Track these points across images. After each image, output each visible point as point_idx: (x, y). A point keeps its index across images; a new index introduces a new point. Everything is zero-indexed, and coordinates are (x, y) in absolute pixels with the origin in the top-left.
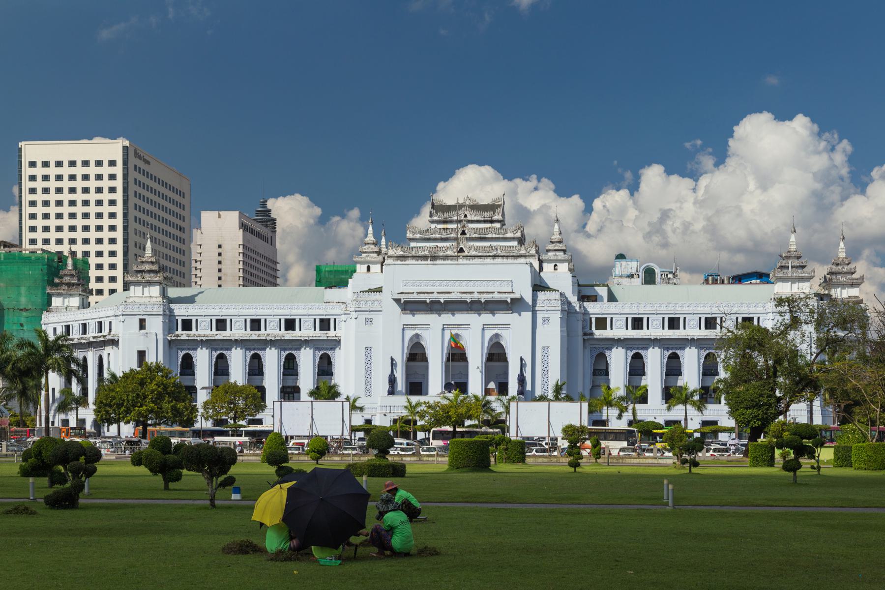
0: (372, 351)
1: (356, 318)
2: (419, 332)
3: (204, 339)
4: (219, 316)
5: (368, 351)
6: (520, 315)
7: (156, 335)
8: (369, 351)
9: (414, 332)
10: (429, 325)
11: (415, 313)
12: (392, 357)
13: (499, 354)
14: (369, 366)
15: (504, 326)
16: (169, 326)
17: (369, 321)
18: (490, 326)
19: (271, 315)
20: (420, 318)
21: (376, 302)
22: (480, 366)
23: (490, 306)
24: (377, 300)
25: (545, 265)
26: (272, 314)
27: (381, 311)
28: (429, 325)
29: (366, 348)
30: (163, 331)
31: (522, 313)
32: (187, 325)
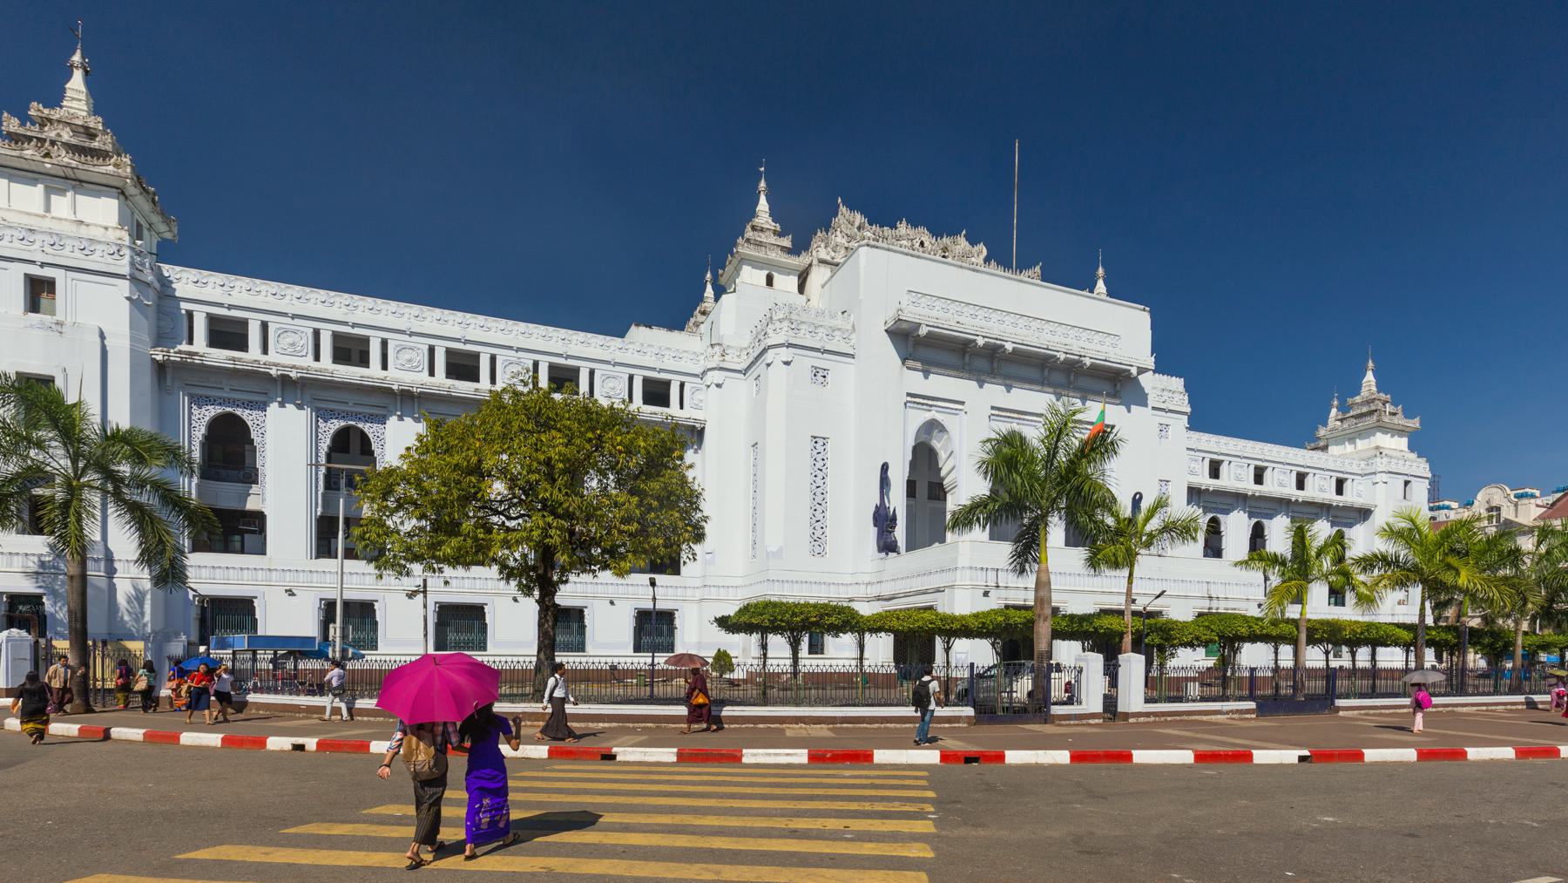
1: (787, 363)
2: (939, 417)
3: (292, 375)
4: (345, 323)
7: (102, 336)
8: (820, 448)
9: (928, 416)
10: (962, 403)
11: (934, 369)
16: (158, 327)
17: (819, 374)
19: (510, 348)
20: (942, 384)
21: (837, 333)
23: (1083, 382)
24: (839, 329)
26: (515, 344)
27: (852, 356)
28: (962, 403)
30: (131, 328)
32: (228, 333)
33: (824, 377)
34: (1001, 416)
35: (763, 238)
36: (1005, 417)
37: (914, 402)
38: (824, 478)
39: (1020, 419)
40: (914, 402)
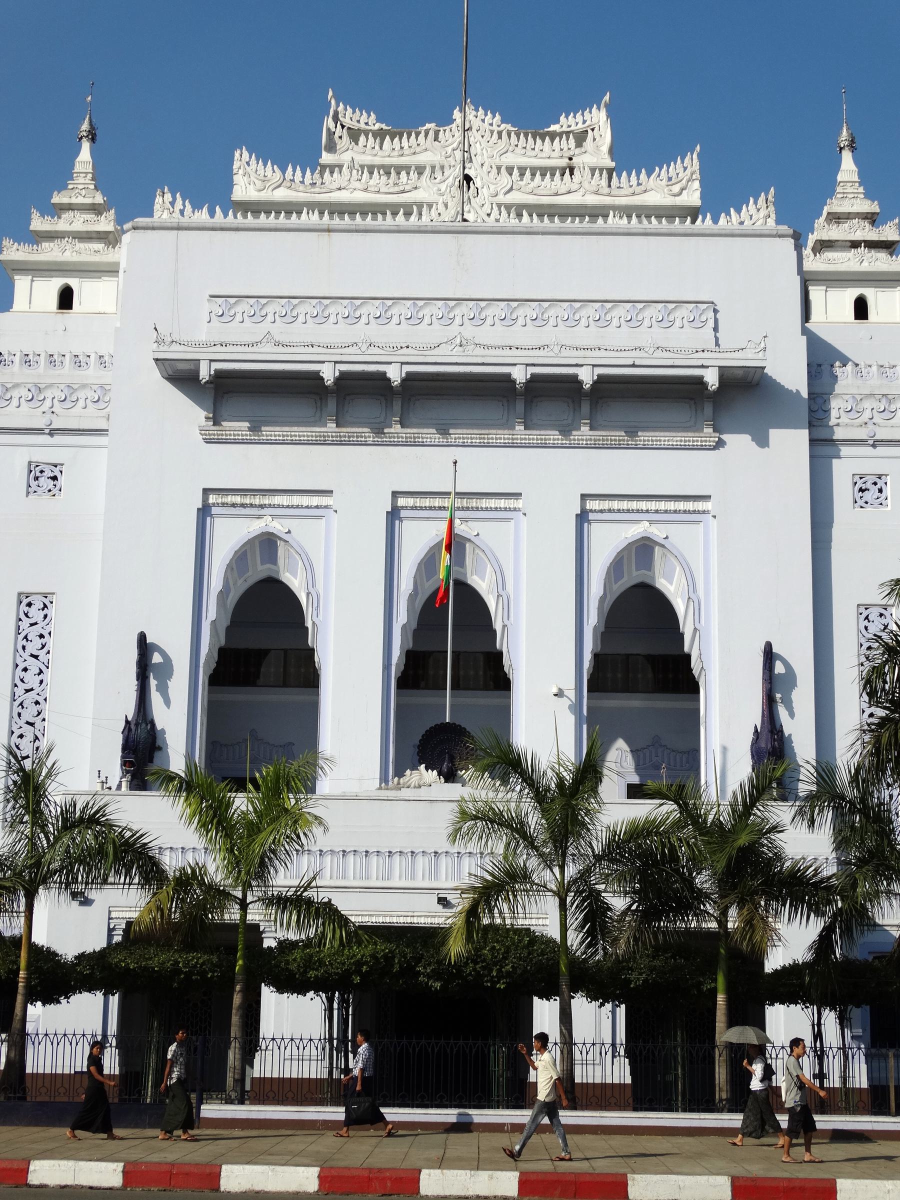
0: (52, 612)
2: (277, 527)
5: (32, 611)
6: (762, 441)
9: (255, 527)
12: (142, 638)
13: (628, 656)
14: (32, 680)
15: (681, 505)
18: (616, 505)
22: (569, 683)
25: (816, 293)
29: (25, 600)
31: (775, 434)
33: (54, 478)
34: (421, 508)
35: (62, 224)
36: (431, 508)
37: (224, 505)
38: (41, 672)
39: (468, 509)
40: (224, 505)
